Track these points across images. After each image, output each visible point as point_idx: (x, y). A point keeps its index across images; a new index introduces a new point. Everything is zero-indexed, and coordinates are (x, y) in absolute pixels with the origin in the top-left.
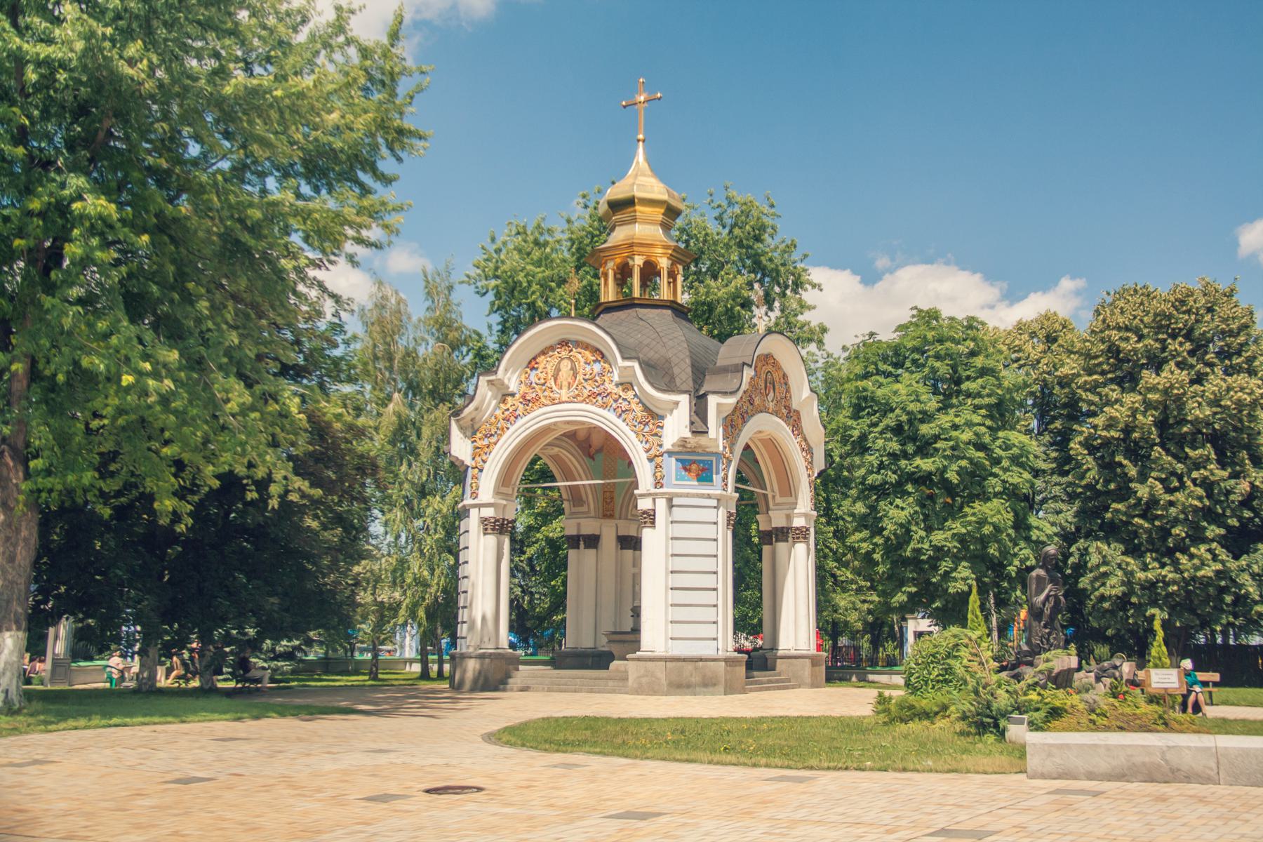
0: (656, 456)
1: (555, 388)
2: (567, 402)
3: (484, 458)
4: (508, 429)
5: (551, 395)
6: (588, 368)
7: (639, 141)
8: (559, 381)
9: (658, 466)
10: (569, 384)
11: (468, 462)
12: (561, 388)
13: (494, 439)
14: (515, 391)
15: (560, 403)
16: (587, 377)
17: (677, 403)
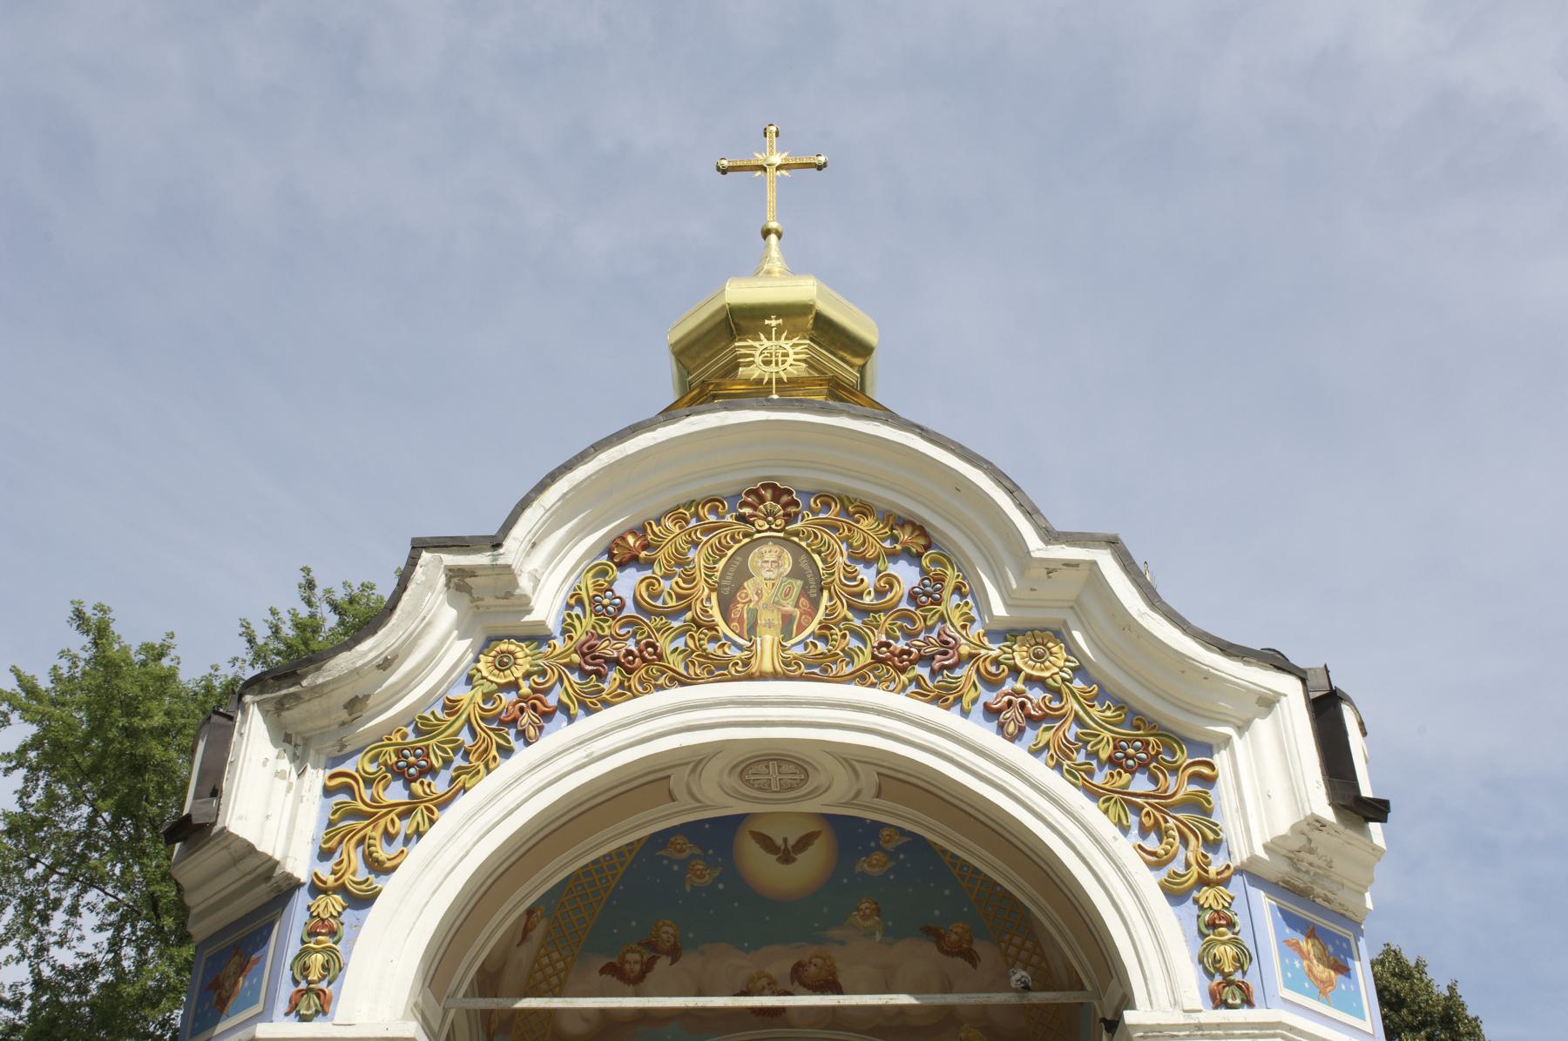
0: (1203, 882)
1: (723, 627)
2: (775, 676)
3: (383, 852)
4: (506, 752)
5: (711, 648)
6: (868, 576)
7: (766, 233)
8: (741, 609)
9: (1216, 923)
10: (787, 619)
11: (300, 864)
12: (753, 629)
13: (440, 785)
14: (553, 625)
15: (751, 677)
16: (867, 600)
17: (1268, 702)
